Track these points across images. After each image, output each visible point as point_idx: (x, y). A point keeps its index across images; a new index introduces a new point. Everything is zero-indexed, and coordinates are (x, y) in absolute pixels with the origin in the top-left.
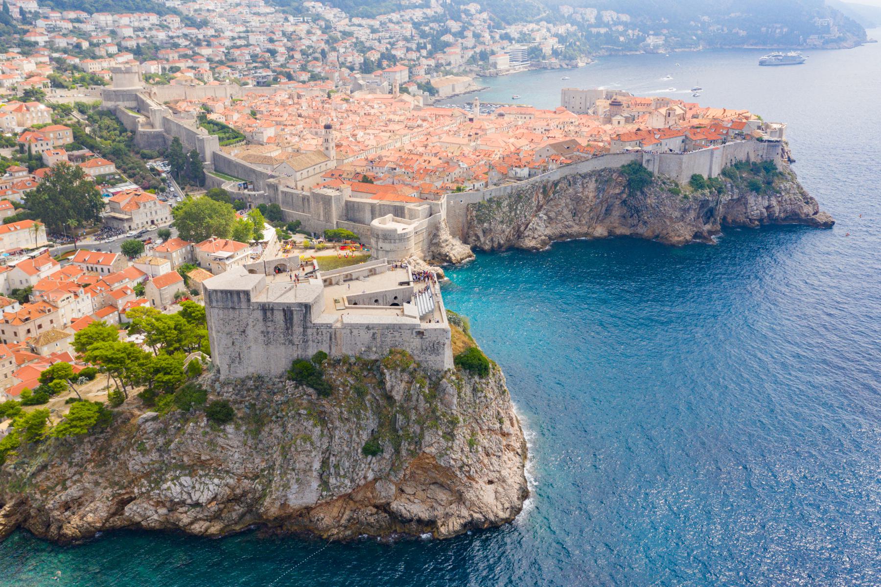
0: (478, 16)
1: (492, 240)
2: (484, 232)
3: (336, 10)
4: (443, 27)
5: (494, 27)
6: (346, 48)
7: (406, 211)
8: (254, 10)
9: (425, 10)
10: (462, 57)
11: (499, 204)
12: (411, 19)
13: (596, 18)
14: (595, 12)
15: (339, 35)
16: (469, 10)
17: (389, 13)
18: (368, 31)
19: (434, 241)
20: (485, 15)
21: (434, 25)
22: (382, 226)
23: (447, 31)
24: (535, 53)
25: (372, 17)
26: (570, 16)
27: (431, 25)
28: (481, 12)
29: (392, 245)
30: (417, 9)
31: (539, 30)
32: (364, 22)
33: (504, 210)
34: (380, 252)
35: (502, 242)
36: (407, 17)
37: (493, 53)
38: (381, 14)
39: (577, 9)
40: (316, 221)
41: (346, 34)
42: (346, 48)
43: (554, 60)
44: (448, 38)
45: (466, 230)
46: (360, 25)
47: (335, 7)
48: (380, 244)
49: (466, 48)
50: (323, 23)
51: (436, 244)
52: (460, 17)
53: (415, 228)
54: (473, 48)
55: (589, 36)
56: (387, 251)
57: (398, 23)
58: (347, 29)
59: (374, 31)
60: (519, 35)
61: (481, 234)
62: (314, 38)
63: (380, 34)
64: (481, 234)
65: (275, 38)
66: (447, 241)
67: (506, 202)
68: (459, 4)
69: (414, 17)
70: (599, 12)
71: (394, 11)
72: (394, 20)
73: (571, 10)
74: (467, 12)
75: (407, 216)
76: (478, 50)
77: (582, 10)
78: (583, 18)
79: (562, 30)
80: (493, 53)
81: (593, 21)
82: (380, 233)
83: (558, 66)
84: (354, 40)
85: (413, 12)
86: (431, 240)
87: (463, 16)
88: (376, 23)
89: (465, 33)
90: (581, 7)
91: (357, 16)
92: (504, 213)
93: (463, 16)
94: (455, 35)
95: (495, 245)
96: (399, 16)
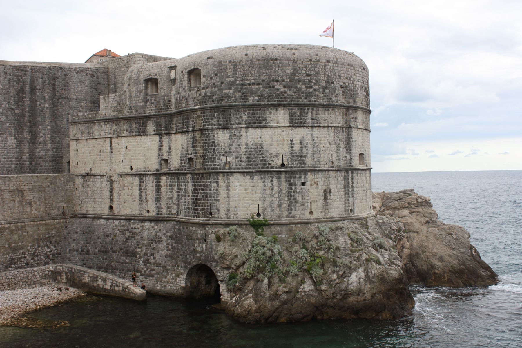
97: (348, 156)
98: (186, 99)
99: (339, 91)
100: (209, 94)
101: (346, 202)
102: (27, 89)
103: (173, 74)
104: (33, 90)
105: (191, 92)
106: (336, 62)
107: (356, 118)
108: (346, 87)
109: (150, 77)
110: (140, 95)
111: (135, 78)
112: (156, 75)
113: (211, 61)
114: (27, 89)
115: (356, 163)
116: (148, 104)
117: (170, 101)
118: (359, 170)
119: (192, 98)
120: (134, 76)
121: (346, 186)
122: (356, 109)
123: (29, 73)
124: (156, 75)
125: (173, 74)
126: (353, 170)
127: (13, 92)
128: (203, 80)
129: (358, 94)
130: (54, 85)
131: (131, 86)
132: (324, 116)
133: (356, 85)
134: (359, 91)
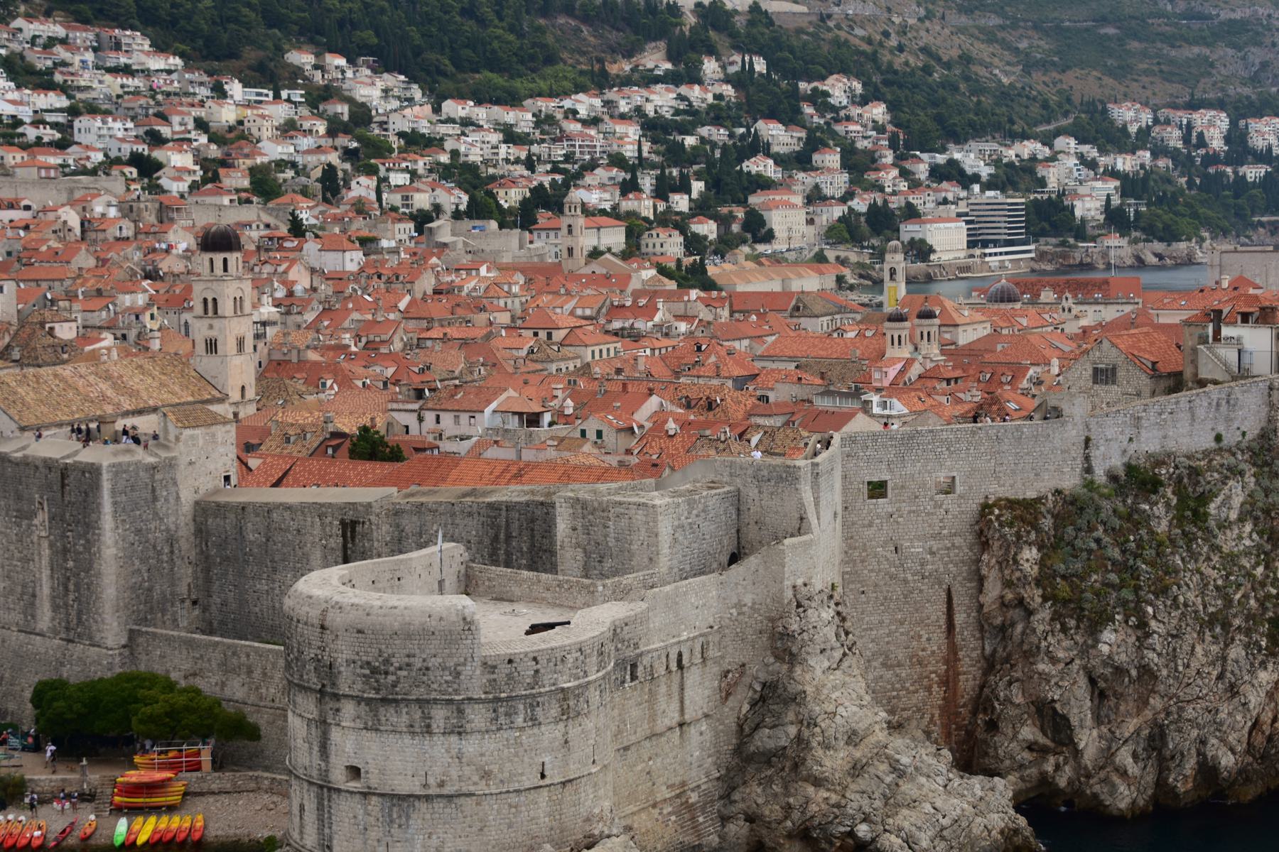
0: (855, 111)
1: (1155, 743)
2: (1101, 693)
3: (395, 80)
4: (743, 137)
5: (909, 146)
6: (414, 174)
7: (562, 526)
8: (114, 59)
9: (683, 90)
10: (810, 222)
11: (1192, 509)
12: (639, 110)
13: (1227, 139)
14: (1223, 121)
15: (395, 142)
16: (826, 94)
17: (567, 94)
18: (495, 138)
19: (765, 740)
20: (878, 111)
21: (719, 134)
22: (351, 596)
23: (758, 147)
24: (1050, 218)
25: (512, 100)
26: (1144, 133)
27: (704, 131)
28: (864, 101)
29: (439, 750)
30: (659, 87)
31: (1053, 158)
32: (481, 114)
33: (1228, 541)
34: (346, 811)
35: (1227, 761)
36: (624, 107)
37: (911, 213)
38: (540, 95)
39: (1164, 113)
40: (15, 638)
41: (414, 141)
42: (414, 174)
43: (1114, 242)
44: (760, 166)
45: (968, 683)
46: (467, 122)
47: (388, 70)
48: (349, 743)
49: (824, 199)
50: (343, 110)
51: (768, 758)
52: (799, 111)
53: (615, 633)
54: (843, 200)
55: (1212, 185)
56: (400, 801)
57: (594, 121)
58: (424, 128)
59: (511, 136)
60: (991, 170)
61: (1079, 708)
62: (306, 142)
63: (535, 148)
64: (1079, 708)
65: (165, 131)
66: (853, 738)
67: (1236, 495)
68: (796, 76)
69: (649, 110)
70: (1233, 123)
71: (579, 88)
72: (583, 112)
73: (1146, 117)
74: (819, 99)
75: (570, 558)
76: (860, 204)
77: (1183, 117)
78: (1186, 139)
79: (1125, 163)
80: (911, 213)
81: (1217, 143)
82: (342, 652)
83: (1129, 262)
84: (444, 158)
85: (645, 93)
86: (744, 731)
87: (808, 110)
88: (522, 119)
89: (816, 157)
90: (1175, 107)
91: (461, 96)
92: (1231, 559)
93: (808, 110)
94: (780, 160)
95: (1183, 779)
96: (597, 102)
97: (323, 764)
99: (310, 667)
101: (320, 830)
102: (502, 536)
104: (509, 537)
106: (306, 624)
107: (338, 710)
108: (319, 660)
114: (502, 536)
115: (338, 776)
118: (339, 791)
121: (320, 807)
122: (337, 697)
123: (504, 513)
126: (330, 789)
127: (487, 541)
129: (340, 672)
130: (532, 530)
132: (299, 699)
133: (335, 660)
134: (342, 669)
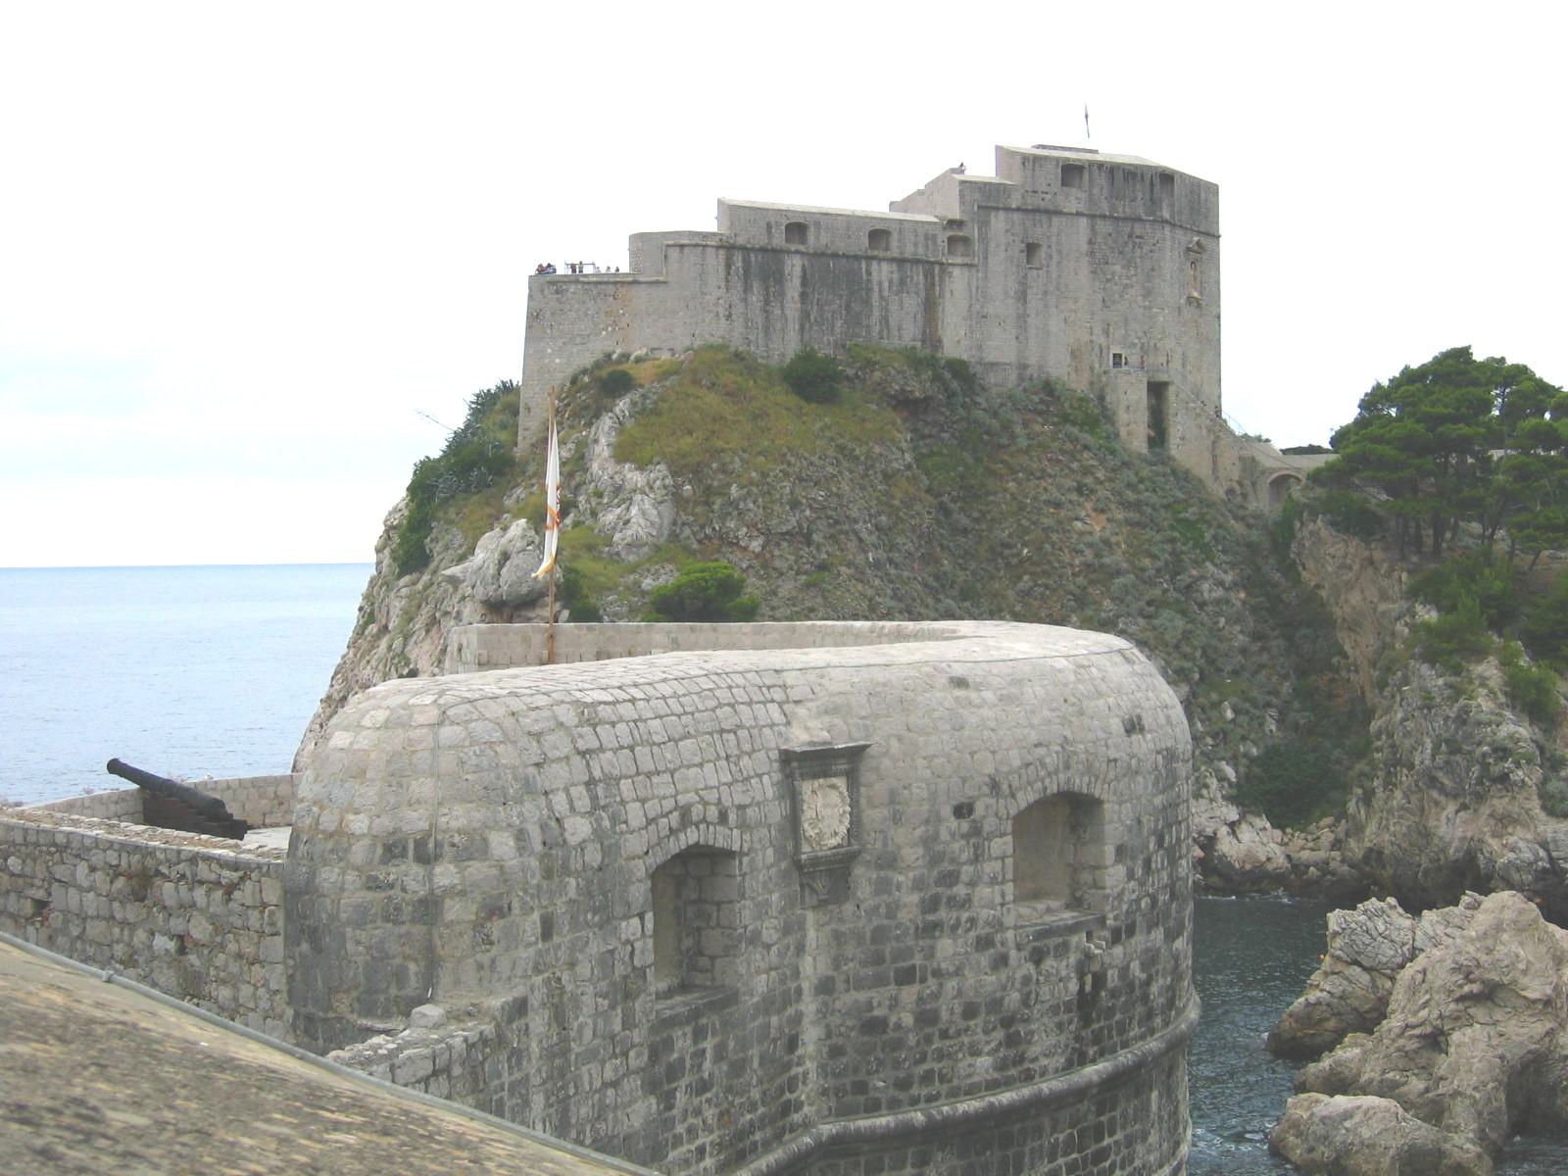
98: (1007, 1022)
100: (1136, 971)
103: (826, 812)
105: (1049, 963)
109: (691, 837)
110: (628, 1024)
111: (593, 856)
112: (723, 818)
113: (1143, 744)
116: (681, 1099)
117: (793, 1043)
119: (1055, 1010)
120: (579, 828)
124: (723, 818)
125: (826, 812)
128: (1115, 875)
131: (563, 937)
